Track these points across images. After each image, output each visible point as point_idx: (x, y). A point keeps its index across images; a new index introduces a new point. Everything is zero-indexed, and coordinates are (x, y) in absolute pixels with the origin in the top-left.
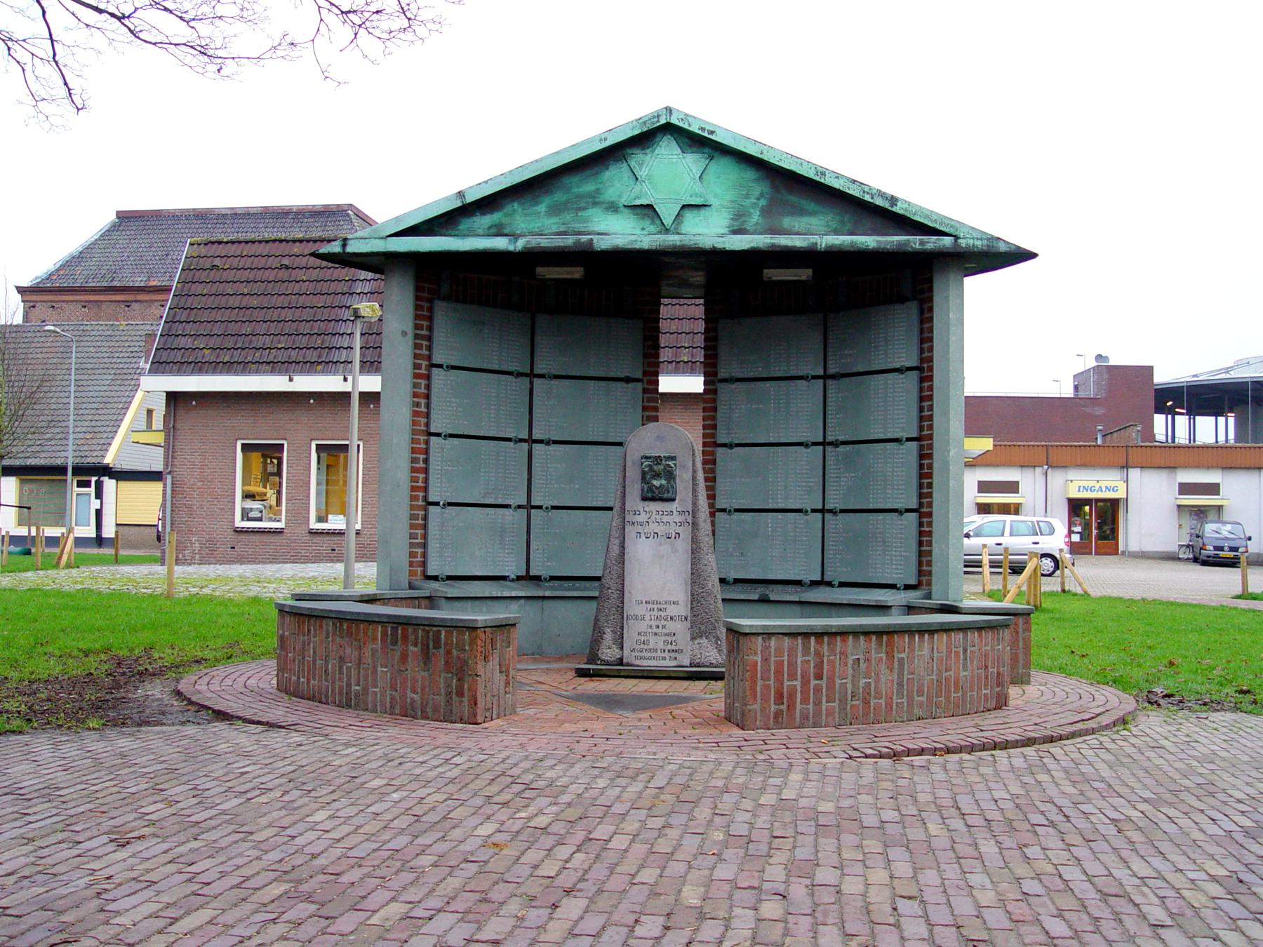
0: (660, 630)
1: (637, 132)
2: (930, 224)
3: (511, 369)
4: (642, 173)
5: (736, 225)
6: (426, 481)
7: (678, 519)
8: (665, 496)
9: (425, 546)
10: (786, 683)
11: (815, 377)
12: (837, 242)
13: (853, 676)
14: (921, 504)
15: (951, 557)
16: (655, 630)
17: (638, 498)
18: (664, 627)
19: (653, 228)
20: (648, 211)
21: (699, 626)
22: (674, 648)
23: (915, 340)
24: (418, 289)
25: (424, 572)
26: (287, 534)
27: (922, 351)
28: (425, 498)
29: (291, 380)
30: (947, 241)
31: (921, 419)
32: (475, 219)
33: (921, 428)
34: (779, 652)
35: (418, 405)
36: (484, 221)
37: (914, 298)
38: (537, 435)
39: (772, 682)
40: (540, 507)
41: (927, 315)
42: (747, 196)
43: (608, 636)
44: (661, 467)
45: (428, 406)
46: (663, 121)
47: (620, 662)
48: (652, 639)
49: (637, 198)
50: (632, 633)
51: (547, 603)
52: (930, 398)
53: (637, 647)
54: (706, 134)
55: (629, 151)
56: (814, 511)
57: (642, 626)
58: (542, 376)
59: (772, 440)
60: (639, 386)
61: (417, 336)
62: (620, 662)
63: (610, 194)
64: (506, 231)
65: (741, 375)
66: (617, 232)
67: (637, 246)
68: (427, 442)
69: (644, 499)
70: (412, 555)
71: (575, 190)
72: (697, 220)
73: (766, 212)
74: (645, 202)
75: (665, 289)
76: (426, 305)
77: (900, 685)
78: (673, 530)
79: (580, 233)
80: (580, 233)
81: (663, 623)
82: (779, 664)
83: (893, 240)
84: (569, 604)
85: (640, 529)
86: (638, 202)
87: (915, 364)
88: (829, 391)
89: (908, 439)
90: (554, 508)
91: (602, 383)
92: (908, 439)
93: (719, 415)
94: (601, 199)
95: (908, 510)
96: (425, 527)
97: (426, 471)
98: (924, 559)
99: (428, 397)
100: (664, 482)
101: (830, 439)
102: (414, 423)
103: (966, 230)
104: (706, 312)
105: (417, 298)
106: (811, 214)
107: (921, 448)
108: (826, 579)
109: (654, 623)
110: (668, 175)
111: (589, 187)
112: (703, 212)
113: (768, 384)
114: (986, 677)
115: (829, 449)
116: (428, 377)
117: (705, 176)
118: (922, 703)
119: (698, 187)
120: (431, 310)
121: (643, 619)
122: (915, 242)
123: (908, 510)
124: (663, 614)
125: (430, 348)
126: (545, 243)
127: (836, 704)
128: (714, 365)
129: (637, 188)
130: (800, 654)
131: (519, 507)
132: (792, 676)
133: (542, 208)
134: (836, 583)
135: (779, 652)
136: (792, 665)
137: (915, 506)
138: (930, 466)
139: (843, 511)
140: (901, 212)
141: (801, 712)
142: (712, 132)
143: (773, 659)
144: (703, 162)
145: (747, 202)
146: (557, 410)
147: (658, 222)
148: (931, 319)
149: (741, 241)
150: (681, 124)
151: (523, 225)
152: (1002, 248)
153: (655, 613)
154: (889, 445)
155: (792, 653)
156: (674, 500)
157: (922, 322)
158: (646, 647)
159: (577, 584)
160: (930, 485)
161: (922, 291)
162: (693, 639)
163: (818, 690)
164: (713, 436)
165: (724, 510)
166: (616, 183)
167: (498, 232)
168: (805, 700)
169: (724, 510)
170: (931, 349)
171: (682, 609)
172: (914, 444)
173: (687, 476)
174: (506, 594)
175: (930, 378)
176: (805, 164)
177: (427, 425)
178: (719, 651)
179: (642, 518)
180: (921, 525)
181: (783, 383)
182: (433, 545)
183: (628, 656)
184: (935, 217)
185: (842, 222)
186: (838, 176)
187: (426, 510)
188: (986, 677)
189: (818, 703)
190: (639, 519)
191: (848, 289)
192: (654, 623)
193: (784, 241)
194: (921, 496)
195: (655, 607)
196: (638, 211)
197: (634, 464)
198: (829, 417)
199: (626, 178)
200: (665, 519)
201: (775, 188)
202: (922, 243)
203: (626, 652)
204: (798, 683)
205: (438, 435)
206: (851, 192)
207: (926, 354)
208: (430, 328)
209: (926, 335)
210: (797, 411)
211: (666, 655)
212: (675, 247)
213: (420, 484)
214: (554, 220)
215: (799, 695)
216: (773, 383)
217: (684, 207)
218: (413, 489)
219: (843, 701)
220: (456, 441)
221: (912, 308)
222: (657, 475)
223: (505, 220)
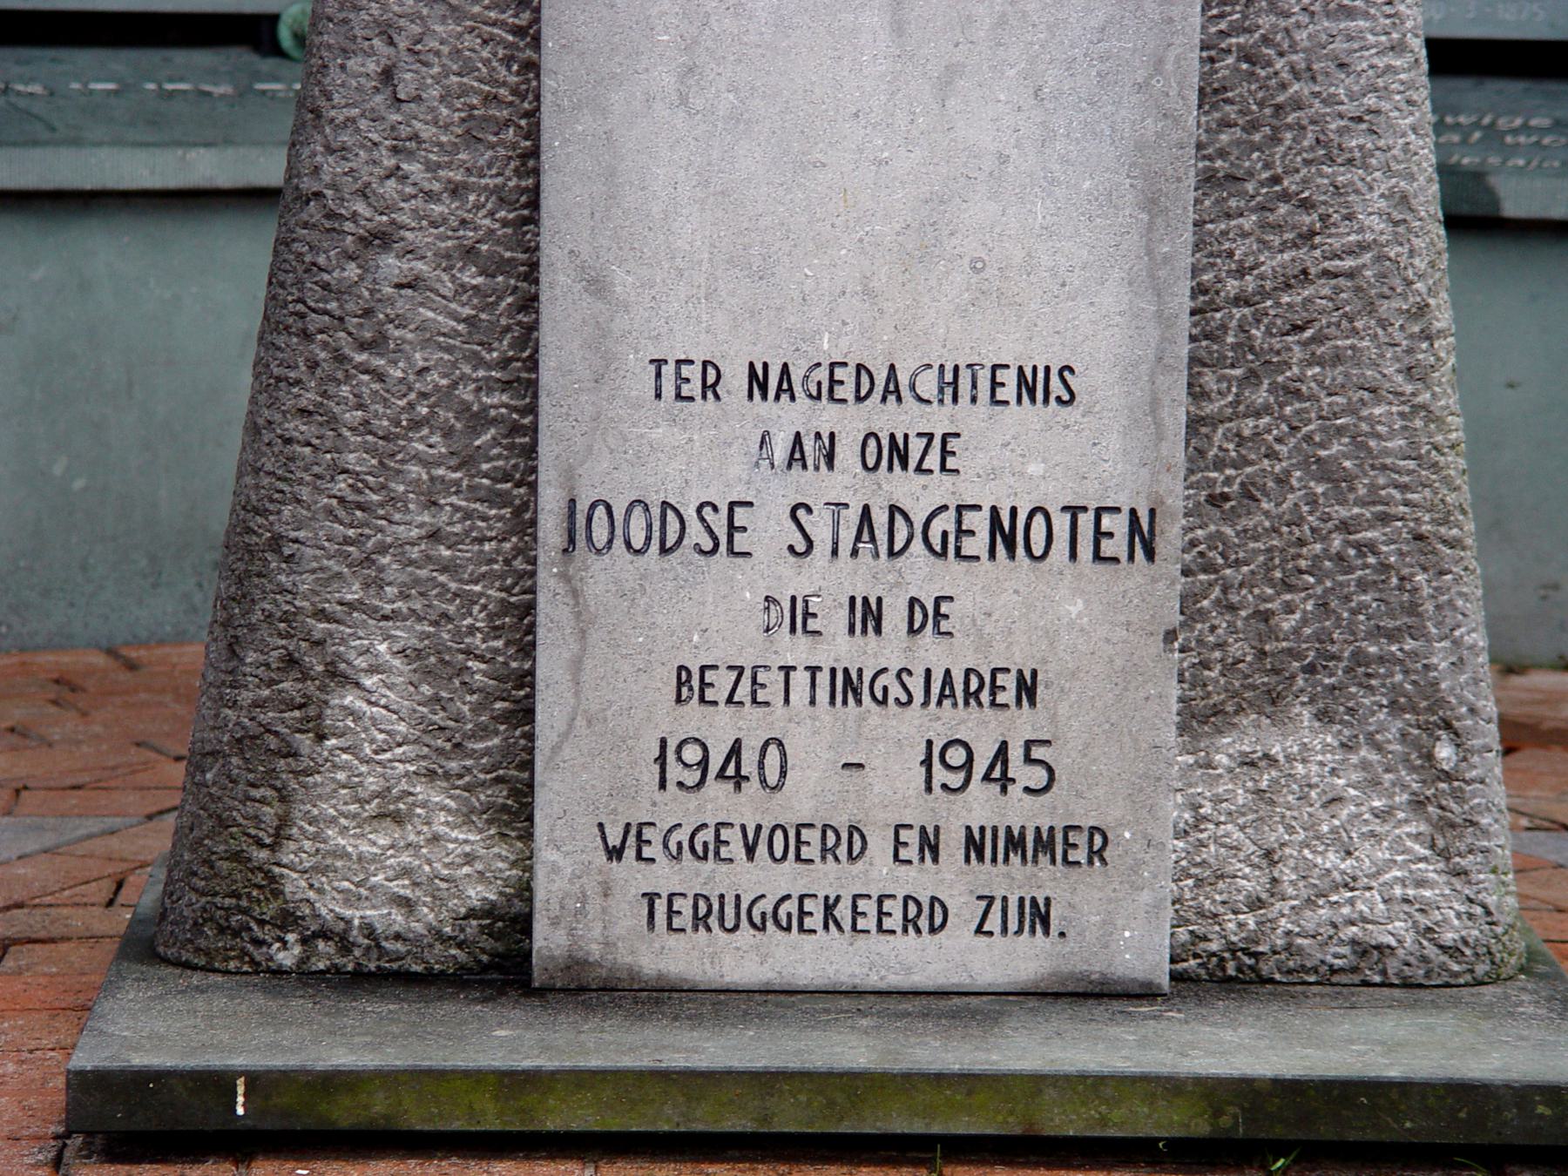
0: (886, 651)
16: (840, 647)
18: (928, 616)
21: (1271, 590)
22: (1020, 812)
43: (381, 699)
47: (499, 960)
48: (814, 734)
50: (616, 667)
53: (678, 811)
57: (719, 612)
62: (499, 960)
81: (921, 575)
109: (832, 582)
121: (727, 541)
124: (918, 493)
153: (846, 482)
158: (746, 808)
162: (1200, 718)
171: (1109, 448)
178: (1449, 834)
183: (584, 905)
192: (832, 582)
195: (849, 423)
203: (563, 860)
211: (952, 880)
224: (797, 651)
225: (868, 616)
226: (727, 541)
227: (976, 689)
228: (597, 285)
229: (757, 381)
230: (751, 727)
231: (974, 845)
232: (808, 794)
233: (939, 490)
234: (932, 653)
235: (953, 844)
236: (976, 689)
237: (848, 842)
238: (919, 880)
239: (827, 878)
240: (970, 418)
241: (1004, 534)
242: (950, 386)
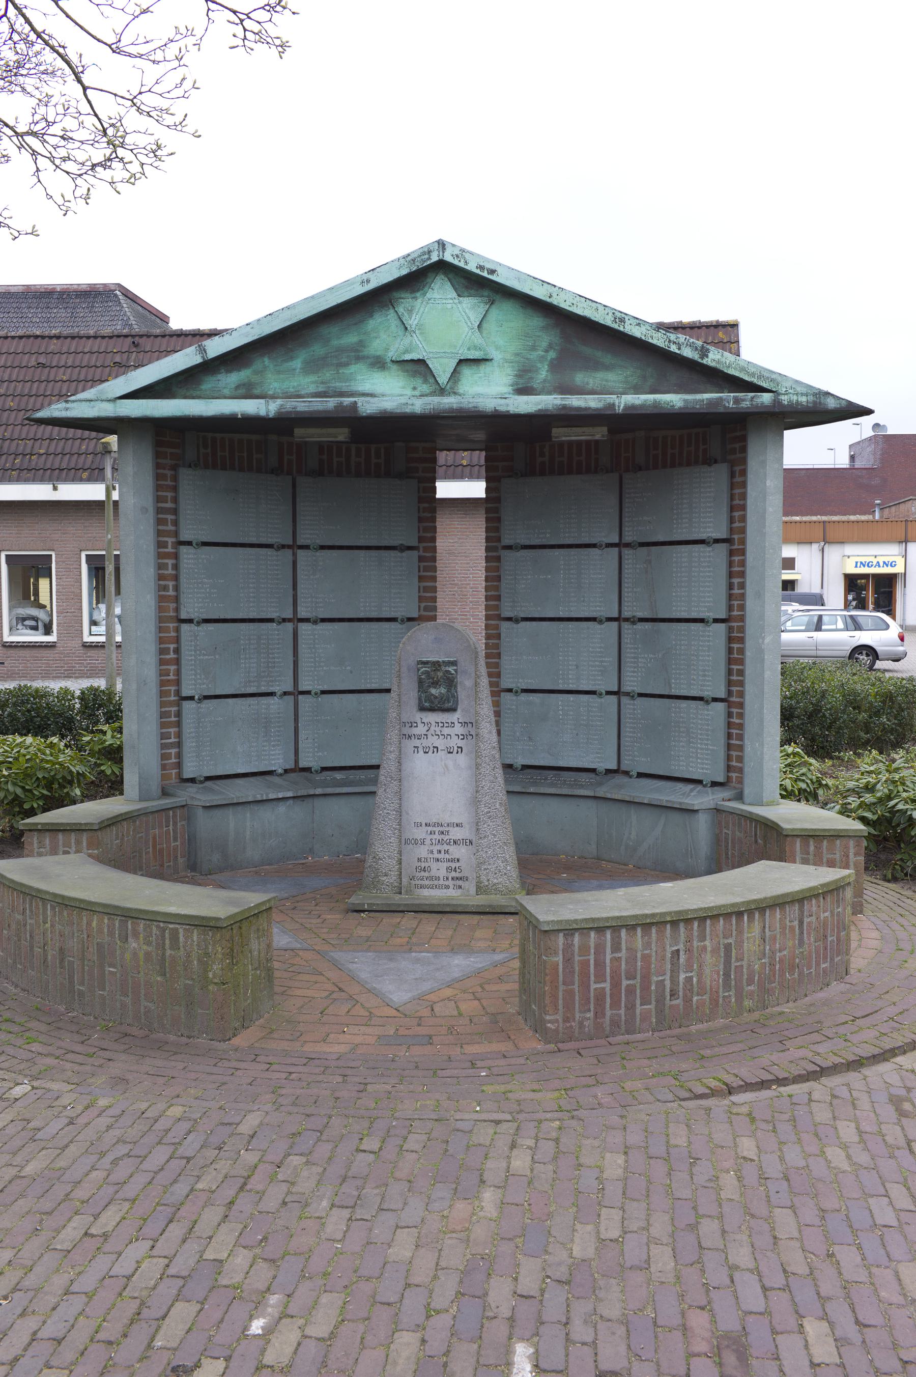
1: (404, 272)
2: (746, 378)
3: (270, 541)
4: (412, 322)
5: (522, 383)
6: (178, 673)
7: (458, 729)
8: (446, 705)
9: (179, 745)
10: (593, 986)
11: (609, 545)
12: (637, 402)
13: (672, 971)
14: (730, 693)
15: (766, 757)
16: (436, 855)
17: (415, 708)
18: (447, 852)
19: (425, 388)
20: (418, 367)
23: (725, 509)
24: (157, 455)
25: (179, 774)
26: (60, 648)
27: (732, 520)
28: (178, 692)
29: (55, 488)
30: (766, 398)
31: (730, 597)
32: (219, 377)
33: (730, 608)
34: (584, 949)
35: (165, 588)
36: (231, 379)
37: (724, 461)
38: (302, 614)
39: (576, 987)
40: (308, 693)
41: (738, 479)
42: (533, 348)
44: (440, 674)
45: (177, 588)
46: (435, 258)
48: (434, 866)
49: (406, 351)
51: (318, 802)
52: (742, 574)
53: (418, 874)
54: (485, 274)
55: (396, 295)
56: (609, 693)
57: (423, 852)
58: (306, 547)
59: (562, 615)
60: (415, 554)
61: (159, 511)
63: (376, 347)
64: (257, 392)
65: (528, 543)
66: (386, 393)
67: (408, 410)
68: (177, 630)
69: (422, 709)
70: (164, 757)
71: (335, 343)
72: (476, 377)
73: (555, 367)
74: (415, 356)
75: (443, 457)
76: (169, 473)
77: (727, 975)
78: (455, 742)
79: (342, 394)
80: (342, 394)
81: (446, 847)
82: (585, 965)
83: (704, 398)
84: (342, 801)
85: (417, 743)
86: (408, 357)
87: (724, 536)
88: (625, 562)
89: (716, 621)
90: (323, 692)
91: (374, 553)
92: (716, 621)
93: (503, 584)
94: (365, 353)
95: (715, 700)
96: (179, 724)
97: (177, 662)
98: (734, 753)
99: (176, 578)
100: (443, 690)
101: (626, 614)
102: (160, 609)
103: (788, 384)
104: (487, 459)
105: (158, 466)
106: (607, 368)
107: (730, 630)
108: (623, 768)
109: (435, 849)
110: (443, 323)
111: (351, 339)
112: (484, 368)
113: (557, 552)
114: (826, 948)
115: (625, 625)
116: (176, 556)
117: (484, 325)
118: (752, 992)
119: (478, 339)
120: (175, 478)
121: (423, 843)
122: (729, 399)
123: (715, 700)
124: (446, 838)
125: (176, 523)
126: (301, 406)
127: (652, 1007)
128: (497, 529)
129: (407, 341)
130: (608, 950)
131: (285, 693)
132: (600, 978)
133: (297, 364)
134: (634, 773)
135: (584, 949)
136: (599, 964)
137: (722, 694)
138: (742, 651)
139: (641, 695)
140: (713, 364)
141: (611, 1020)
142: (492, 272)
143: (577, 958)
144: (482, 308)
145: (534, 355)
146: (325, 584)
147: (431, 380)
148: (744, 485)
149: (527, 403)
150: (456, 262)
151: (276, 385)
152: (831, 404)
154: (693, 626)
156: (454, 710)
157: (732, 486)
158: (426, 874)
159: (352, 775)
160: (741, 673)
161: (733, 451)
163: (630, 990)
164: (497, 608)
165: (510, 690)
166: (383, 333)
167: (247, 392)
168: (615, 1004)
169: (510, 690)
170: (743, 519)
172: (722, 627)
173: (469, 683)
174: (271, 796)
175: (743, 552)
176: (601, 308)
177: (177, 610)
179: (421, 730)
180: (730, 715)
181: (573, 551)
182: (189, 745)
184: (753, 370)
185: (644, 378)
186: (640, 322)
187: (179, 705)
188: (826, 948)
189: (631, 1007)
190: (416, 731)
191: (650, 441)
193: (576, 401)
194: (730, 683)
195: (437, 829)
196: (410, 367)
197: (409, 670)
198: (624, 590)
199: (393, 328)
200: (446, 731)
202: (737, 401)
204: (607, 985)
205: (190, 621)
206: (655, 342)
207: (737, 525)
208: (175, 500)
209: (737, 502)
210: (590, 584)
211: (450, 883)
212: (452, 410)
213: (172, 677)
214: (312, 378)
215: (608, 1000)
216: (562, 551)
217: (461, 361)
218: (162, 683)
219: (660, 1001)
220: (211, 627)
221: (720, 472)
222: (435, 684)
223: (255, 379)
224: (431, 856)
225: (440, 852)
226: (423, 843)
227: (452, 860)
228: (408, 814)
229: (426, 825)
230: (427, 865)
231: (452, 879)
232: (434, 873)
233: (447, 837)
234: (447, 856)
235: (450, 879)
236: (452, 860)
237: (438, 878)
238: (446, 883)
239: (436, 882)
240: (450, 829)
241: (455, 842)
242: (448, 825)
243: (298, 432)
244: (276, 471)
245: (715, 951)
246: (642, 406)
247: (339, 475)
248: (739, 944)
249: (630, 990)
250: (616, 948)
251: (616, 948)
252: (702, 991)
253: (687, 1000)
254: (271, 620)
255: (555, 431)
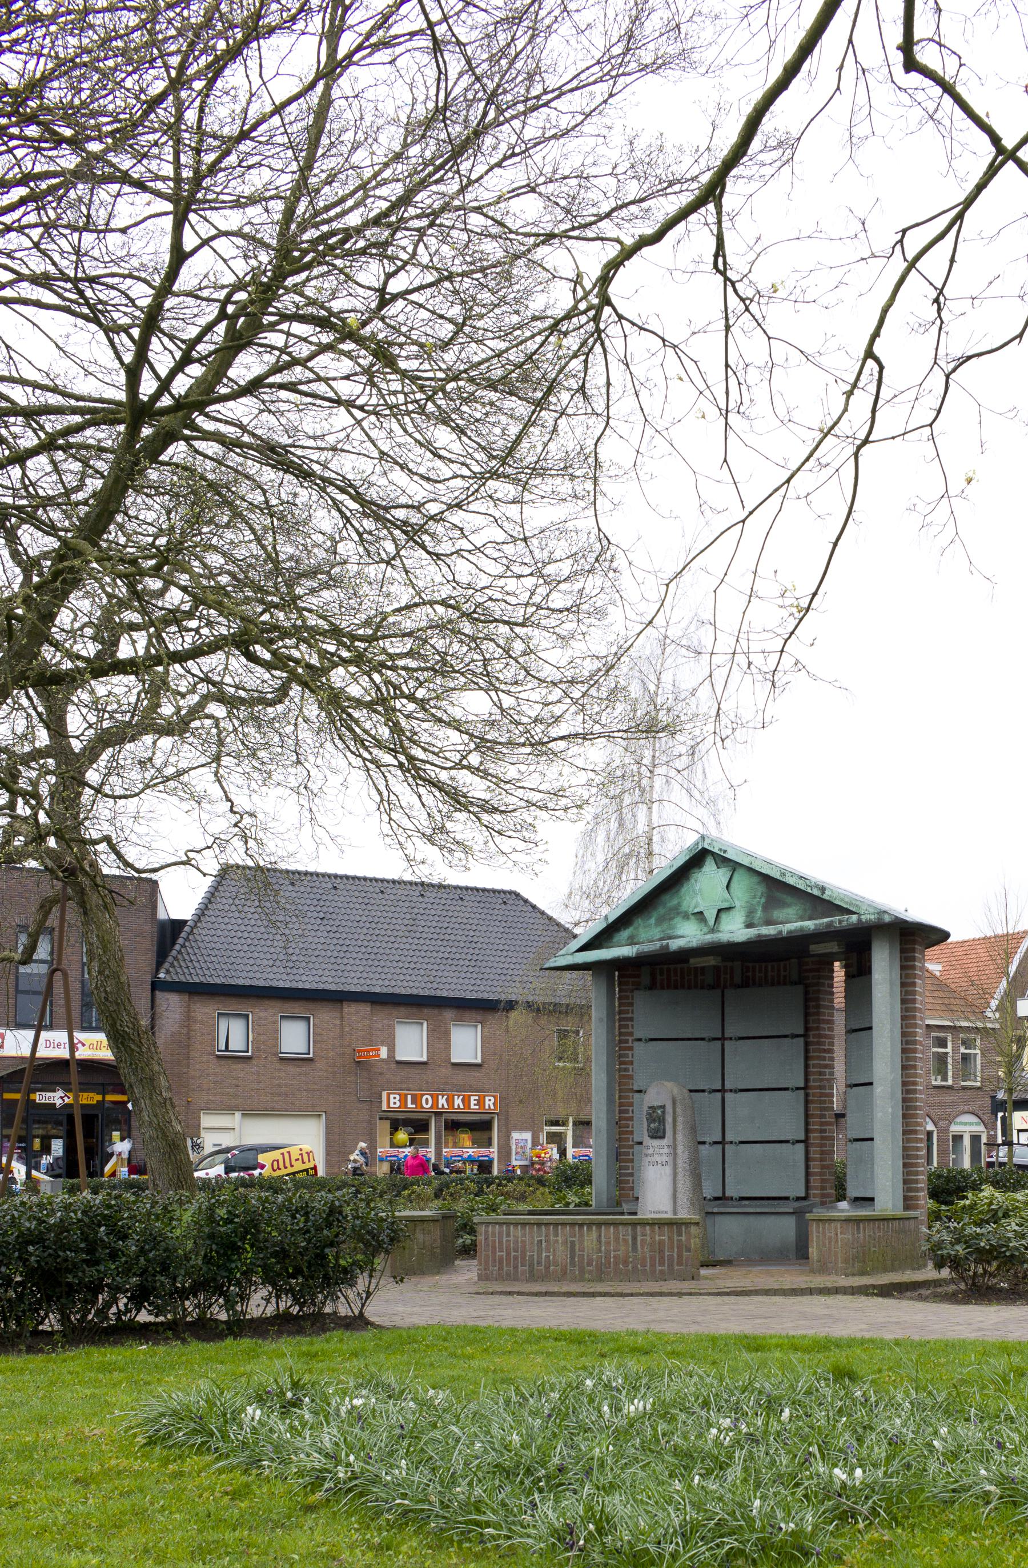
30: (854, 918)
34: (493, 1233)
36: (625, 934)
42: (754, 897)
66: (689, 935)
73: (766, 908)
77: (572, 1258)
106: (788, 906)
110: (708, 887)
111: (675, 902)
112: (732, 912)
133: (653, 921)
135: (493, 1233)
136: (501, 1242)
155: (500, 1234)
163: (516, 1258)
168: (508, 1265)
186: (793, 874)
189: (516, 1267)
201: (769, 888)
202: (840, 922)
204: (504, 1254)
219: (531, 1265)
243: (692, 961)
244: (711, 987)
245: (565, 1242)
246: (795, 931)
247: (760, 985)
248: (581, 1242)
249: (516, 1258)
250: (508, 1235)
251: (508, 1235)
252: (556, 1264)
253: (547, 1268)
254: (703, 1091)
255: (812, 947)
